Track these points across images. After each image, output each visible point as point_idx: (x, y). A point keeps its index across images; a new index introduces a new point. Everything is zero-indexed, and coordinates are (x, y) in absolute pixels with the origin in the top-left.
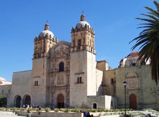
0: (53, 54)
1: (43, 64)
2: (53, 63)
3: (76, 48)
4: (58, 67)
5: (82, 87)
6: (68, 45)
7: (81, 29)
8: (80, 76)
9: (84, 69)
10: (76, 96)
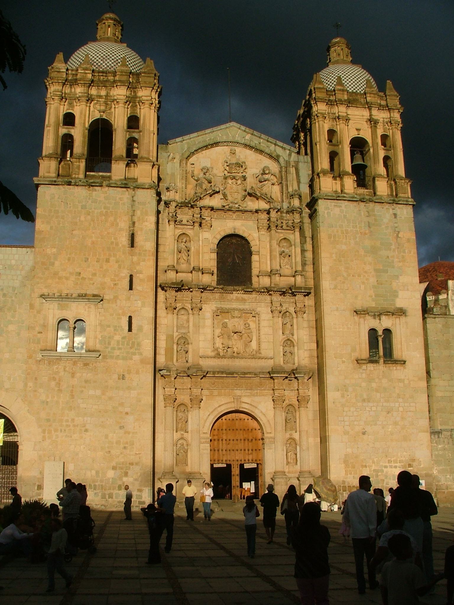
0: (179, 184)
1: (124, 224)
2: (178, 232)
3: (350, 183)
4: (214, 256)
5: (400, 381)
6: (276, 158)
7: (369, 99)
8: (386, 322)
9: (401, 294)
10: (368, 429)
